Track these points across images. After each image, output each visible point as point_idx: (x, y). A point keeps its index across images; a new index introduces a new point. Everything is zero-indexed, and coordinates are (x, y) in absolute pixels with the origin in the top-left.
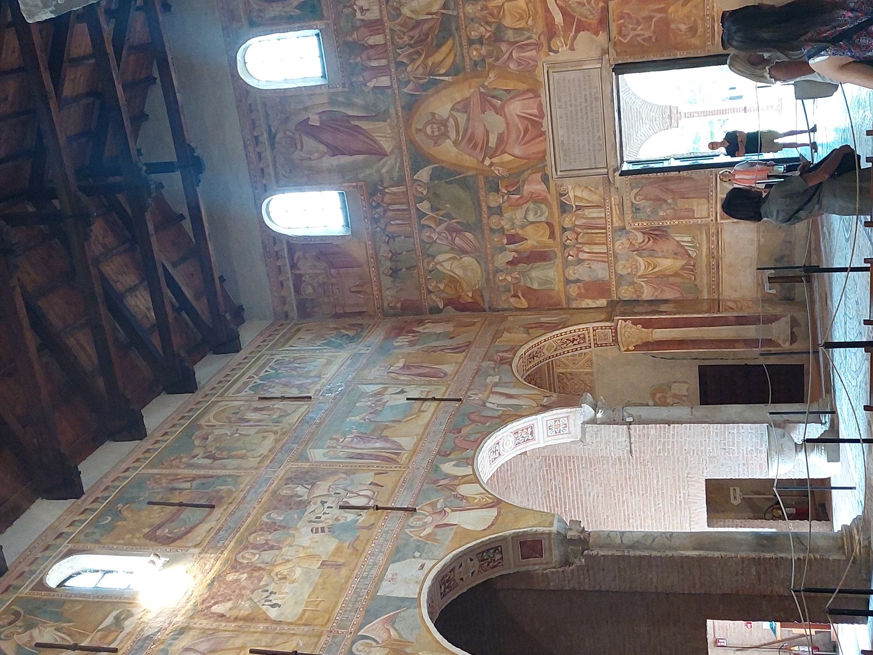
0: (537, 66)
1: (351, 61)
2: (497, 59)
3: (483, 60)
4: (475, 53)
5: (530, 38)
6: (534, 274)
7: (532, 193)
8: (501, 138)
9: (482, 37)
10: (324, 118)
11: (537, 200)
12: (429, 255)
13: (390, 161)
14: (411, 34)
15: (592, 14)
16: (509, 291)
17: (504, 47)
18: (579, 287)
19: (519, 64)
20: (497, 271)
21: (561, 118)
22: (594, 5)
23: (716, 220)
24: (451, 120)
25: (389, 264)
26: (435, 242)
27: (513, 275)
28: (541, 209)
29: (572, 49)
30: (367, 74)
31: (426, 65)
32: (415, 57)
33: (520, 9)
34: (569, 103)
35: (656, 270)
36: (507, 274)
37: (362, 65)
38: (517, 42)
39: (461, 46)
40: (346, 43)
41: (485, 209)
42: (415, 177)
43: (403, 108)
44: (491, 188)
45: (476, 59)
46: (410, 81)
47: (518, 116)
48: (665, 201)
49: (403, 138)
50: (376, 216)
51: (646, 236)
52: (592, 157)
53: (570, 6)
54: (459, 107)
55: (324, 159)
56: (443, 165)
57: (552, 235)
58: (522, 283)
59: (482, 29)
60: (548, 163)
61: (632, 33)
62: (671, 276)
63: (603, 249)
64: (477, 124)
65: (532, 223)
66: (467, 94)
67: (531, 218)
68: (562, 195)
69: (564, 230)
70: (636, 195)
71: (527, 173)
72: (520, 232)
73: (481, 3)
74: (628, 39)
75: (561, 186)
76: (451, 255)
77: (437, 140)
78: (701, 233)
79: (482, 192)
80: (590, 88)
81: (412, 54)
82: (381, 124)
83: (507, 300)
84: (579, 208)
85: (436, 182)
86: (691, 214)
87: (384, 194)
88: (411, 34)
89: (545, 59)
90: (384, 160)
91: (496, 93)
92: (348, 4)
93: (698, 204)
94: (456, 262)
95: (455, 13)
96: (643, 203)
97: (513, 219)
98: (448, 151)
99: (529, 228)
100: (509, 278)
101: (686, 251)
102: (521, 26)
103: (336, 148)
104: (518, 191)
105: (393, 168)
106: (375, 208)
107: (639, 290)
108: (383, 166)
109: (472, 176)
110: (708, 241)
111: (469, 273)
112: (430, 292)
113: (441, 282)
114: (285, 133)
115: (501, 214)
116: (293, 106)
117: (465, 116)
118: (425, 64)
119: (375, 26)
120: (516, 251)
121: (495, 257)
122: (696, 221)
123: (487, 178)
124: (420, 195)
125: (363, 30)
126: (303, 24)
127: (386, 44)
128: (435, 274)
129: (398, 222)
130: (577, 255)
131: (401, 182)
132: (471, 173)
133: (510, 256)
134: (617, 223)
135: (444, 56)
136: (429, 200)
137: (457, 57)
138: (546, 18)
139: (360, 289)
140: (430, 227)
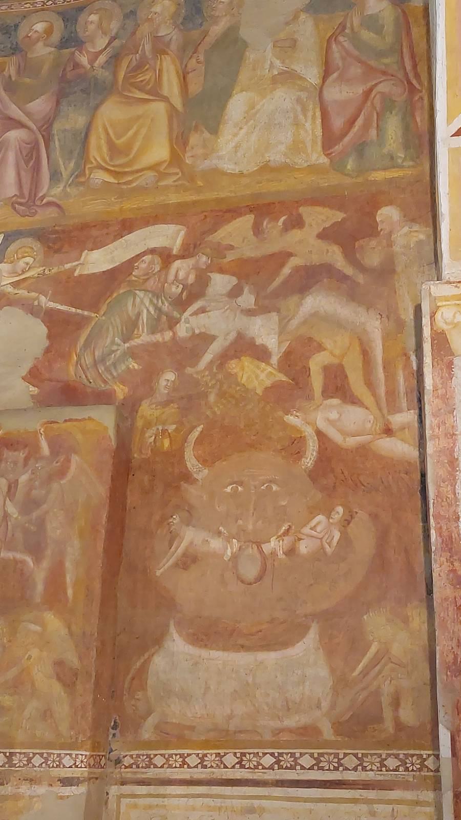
3: (15, 50)
4: (40, 27)
5: (55, 176)
15: (95, 364)
17: (40, 105)
45: (22, 32)
59: (101, 43)
102: (93, 153)
138: (105, 224)
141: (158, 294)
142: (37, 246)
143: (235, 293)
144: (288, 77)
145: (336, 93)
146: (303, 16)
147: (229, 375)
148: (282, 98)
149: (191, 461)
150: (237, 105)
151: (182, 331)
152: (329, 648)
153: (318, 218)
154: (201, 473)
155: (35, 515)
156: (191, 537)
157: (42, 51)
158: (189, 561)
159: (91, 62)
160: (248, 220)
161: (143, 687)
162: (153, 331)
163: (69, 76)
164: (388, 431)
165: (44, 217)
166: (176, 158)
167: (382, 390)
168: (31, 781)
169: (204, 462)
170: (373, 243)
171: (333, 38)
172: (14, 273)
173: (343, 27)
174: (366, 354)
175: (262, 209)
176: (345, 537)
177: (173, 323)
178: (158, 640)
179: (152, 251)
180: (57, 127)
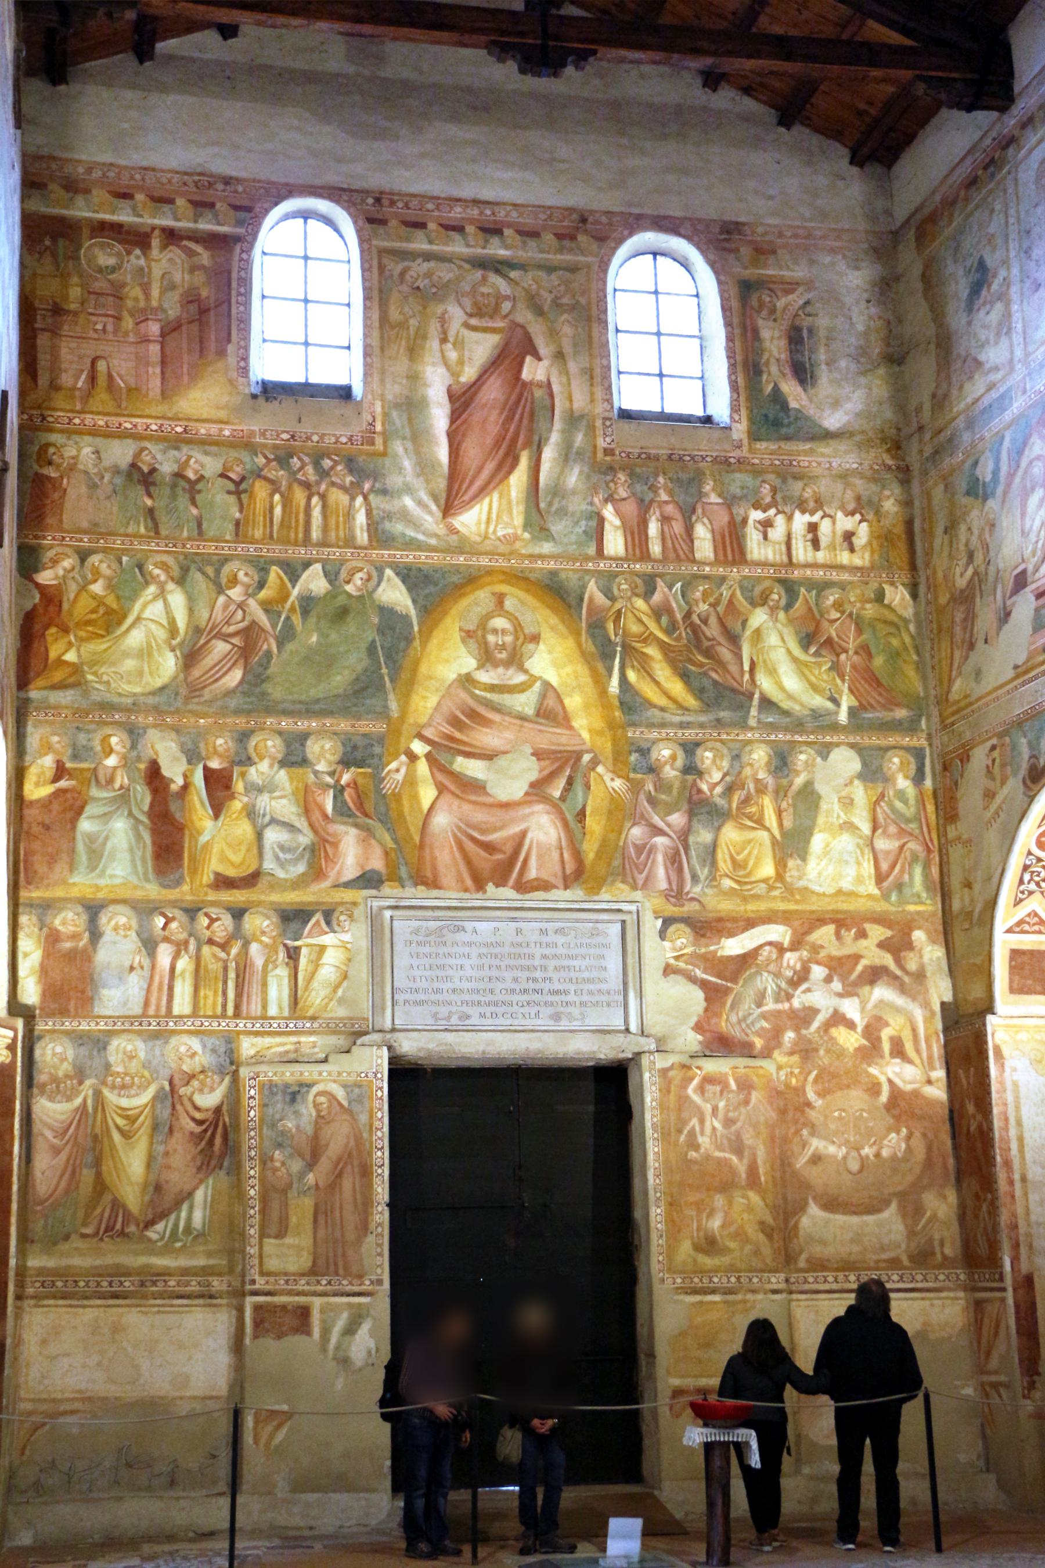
0: (634, 887)
1: (661, 479)
2: (652, 801)
4: (666, 753)
5: (695, 878)
6: (120, 826)
7: (335, 845)
8: (477, 787)
9: (700, 774)
10: (538, 393)
11: (319, 855)
12: (185, 570)
13: (430, 520)
14: (713, 621)
15: (739, 1022)
16: (75, 757)
17: (677, 819)
18: (75, 936)
19: (640, 849)
20: (134, 734)
21: (519, 931)
22: (758, 1026)
23: (255, 1293)
24: (520, 678)
25: (167, 468)
26: (220, 591)
27: (119, 772)
28: (296, 861)
29: (668, 970)
30: (630, 508)
31: (645, 641)
32: (664, 620)
33: (756, 865)
34: (548, 951)
35: (116, 1137)
36: (124, 757)
37: (652, 501)
38: (686, 848)
39: (682, 726)
40: (698, 478)
41: (302, 725)
42: (389, 572)
43: (554, 573)
44: (355, 747)
45: (654, 755)
46: (613, 599)
47: (524, 834)
48: (311, 1166)
49: (484, 561)
50: (295, 462)
51: (209, 1115)
52: (421, 997)
53: (758, 973)
54: (551, 702)
55: (441, 370)
56: (417, 643)
57: (223, 882)
58: (94, 792)
59: (717, 776)
60: (410, 891)
61: (707, 1108)
62: (99, 1174)
63: (182, 1003)
64: (509, 735)
65: (259, 836)
66: (582, 723)
67: (273, 836)
68: (328, 915)
69: (238, 914)
70: (331, 1097)
71: (387, 838)
72: (237, 805)
73: (770, 781)
74: (696, 1098)
75: (351, 916)
76: (181, 622)
77: (475, 636)
78: (209, 1254)
79: (343, 725)
80: (583, 1004)
81: (670, 611)
82: (519, 520)
83: (49, 748)
84: (293, 955)
85: (376, 621)
86: (273, 1229)
87: (352, 491)
88: (713, 621)
89: (647, 907)
90: (434, 508)
91: (579, 788)
92: (778, 497)
93: (299, 1249)
94: (161, 634)
95: (752, 722)
96: (307, 1111)
97: (271, 788)
98: (448, 661)
99: (244, 829)
100: (111, 761)
101: (163, 1215)
102: (721, 864)
103: (466, 405)
104: (342, 810)
105: (417, 526)
106: (317, 465)
107: (58, 1089)
108: (420, 503)
109: (386, 707)
110: (185, 1272)
111: (130, 664)
112: (83, 556)
113: (110, 587)
114: (507, 298)
115: (284, 763)
116: (567, 330)
117: (530, 711)
118: (647, 638)
119: (731, 544)
120: (186, 787)
121: (173, 735)
122: (254, 1241)
123: (381, 740)
124: (343, 575)
125: (722, 518)
126: (742, 391)
127: (694, 561)
128: (134, 577)
129: (278, 511)
130: (166, 940)
131: (379, 536)
132: (393, 705)
133: (174, 771)
134: (247, 1047)
135: (664, 684)
136: (331, 595)
137: (657, 712)
138: (734, 920)
139: (102, 380)
140: (261, 585)
141: (777, 975)
142: (688, 930)
143: (828, 980)
144: (849, 827)
145: (883, 844)
146: (856, 782)
147: (832, 1039)
148: (846, 842)
149: (811, 1095)
150: (818, 841)
151: (796, 1003)
152: (903, 1211)
153: (877, 933)
154: (819, 1103)
155: (733, 1128)
156: (816, 1144)
157: (670, 773)
158: (816, 1159)
159: (711, 790)
160: (830, 929)
161: (796, 1236)
162: (777, 1000)
163: (695, 797)
164: (929, 1082)
165: (689, 908)
166: (780, 876)
167: (925, 1055)
168: (754, 1291)
169: (820, 1094)
170: (911, 955)
171: (877, 802)
172: (674, 949)
173: (882, 796)
174: (914, 1030)
175: (841, 922)
176: (908, 1146)
177: (789, 997)
178: (802, 1208)
179: (770, 943)
180: (691, 840)
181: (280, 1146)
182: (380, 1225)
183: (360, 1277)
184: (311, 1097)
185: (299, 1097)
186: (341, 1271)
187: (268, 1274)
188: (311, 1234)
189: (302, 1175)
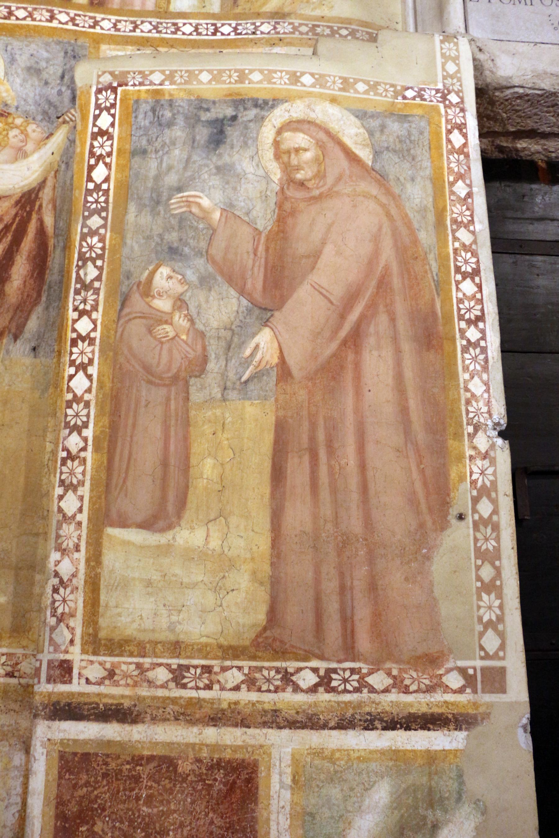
70: (328, 139)
86: (140, 496)
181: (173, 253)
182: (485, 492)
183: (431, 661)
184: (268, 133)
185: (233, 134)
186: (364, 642)
187: (117, 646)
188: (263, 520)
189: (235, 337)
